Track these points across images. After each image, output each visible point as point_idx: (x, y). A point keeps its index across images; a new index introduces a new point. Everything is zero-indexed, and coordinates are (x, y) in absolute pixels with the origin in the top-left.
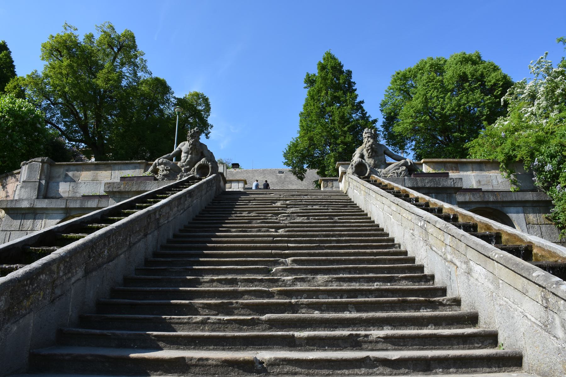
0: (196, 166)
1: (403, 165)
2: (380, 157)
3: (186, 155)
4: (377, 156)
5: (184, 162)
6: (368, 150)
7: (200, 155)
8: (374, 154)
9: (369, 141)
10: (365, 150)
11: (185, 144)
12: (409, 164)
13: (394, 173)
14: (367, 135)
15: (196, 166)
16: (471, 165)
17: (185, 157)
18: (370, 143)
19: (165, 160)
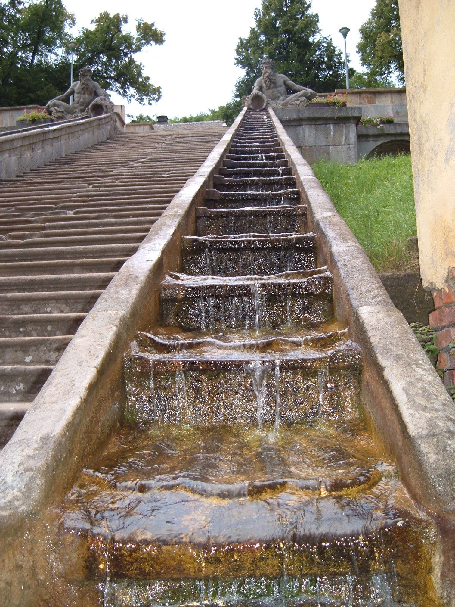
0: (90, 106)
1: (302, 96)
2: (279, 89)
3: (79, 95)
4: (276, 87)
5: (78, 102)
6: (266, 81)
7: (93, 94)
8: (272, 86)
9: (267, 72)
10: (263, 82)
11: (77, 84)
12: (309, 94)
13: (292, 104)
14: (265, 65)
15: (90, 106)
16: (389, 95)
17: (77, 97)
18: (267, 74)
19: (58, 102)
